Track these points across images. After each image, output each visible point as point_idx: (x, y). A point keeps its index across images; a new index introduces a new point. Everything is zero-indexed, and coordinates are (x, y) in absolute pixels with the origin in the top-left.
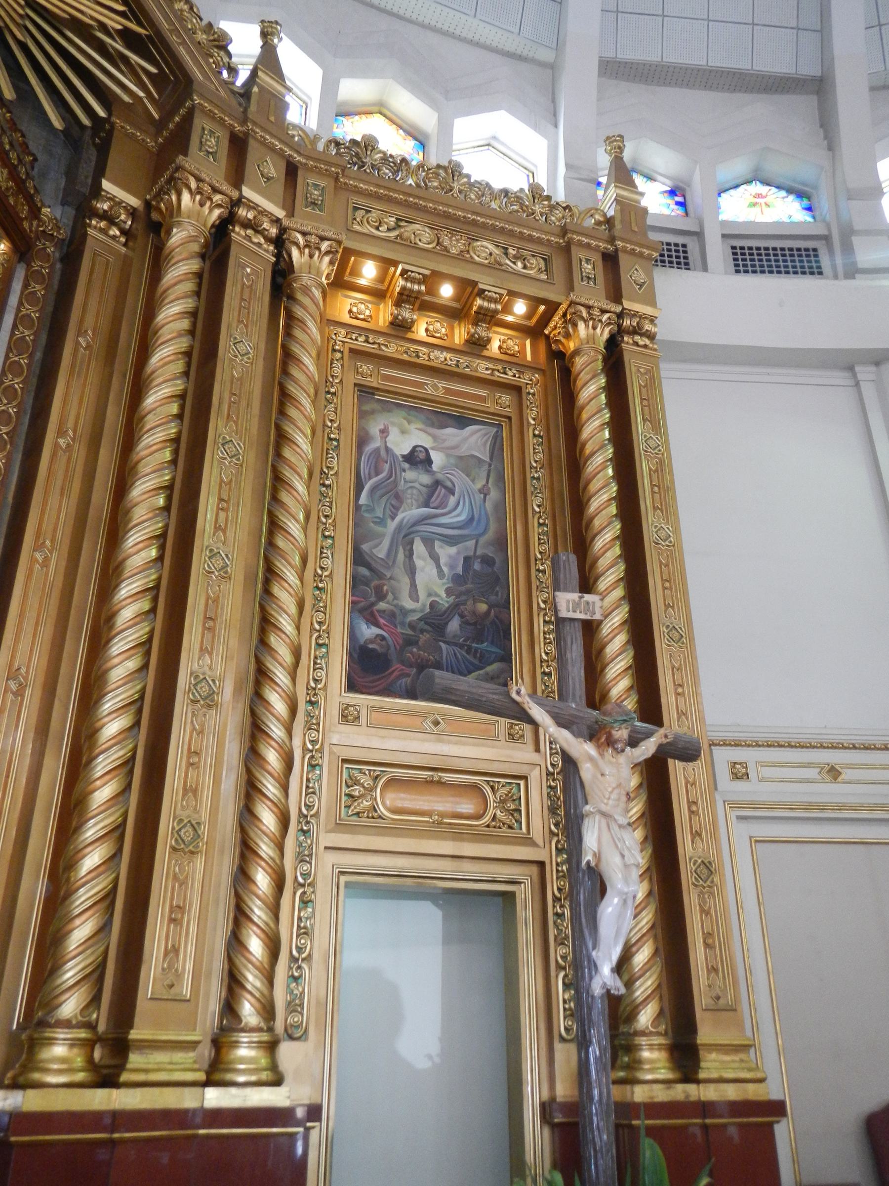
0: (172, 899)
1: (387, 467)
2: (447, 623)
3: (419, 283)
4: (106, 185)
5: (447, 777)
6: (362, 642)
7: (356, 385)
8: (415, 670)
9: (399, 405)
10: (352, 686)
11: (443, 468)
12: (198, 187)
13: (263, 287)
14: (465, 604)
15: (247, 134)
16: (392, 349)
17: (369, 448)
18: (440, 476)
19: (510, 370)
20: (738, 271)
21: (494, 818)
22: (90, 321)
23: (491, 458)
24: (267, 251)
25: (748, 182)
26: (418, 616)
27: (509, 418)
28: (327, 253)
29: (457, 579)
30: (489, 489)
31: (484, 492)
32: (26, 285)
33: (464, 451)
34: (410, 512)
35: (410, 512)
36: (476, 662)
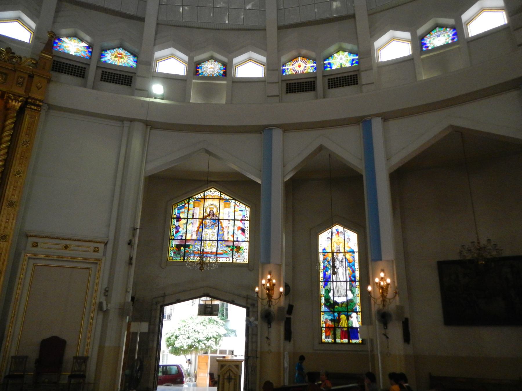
20: (101, 80)
25: (118, 48)
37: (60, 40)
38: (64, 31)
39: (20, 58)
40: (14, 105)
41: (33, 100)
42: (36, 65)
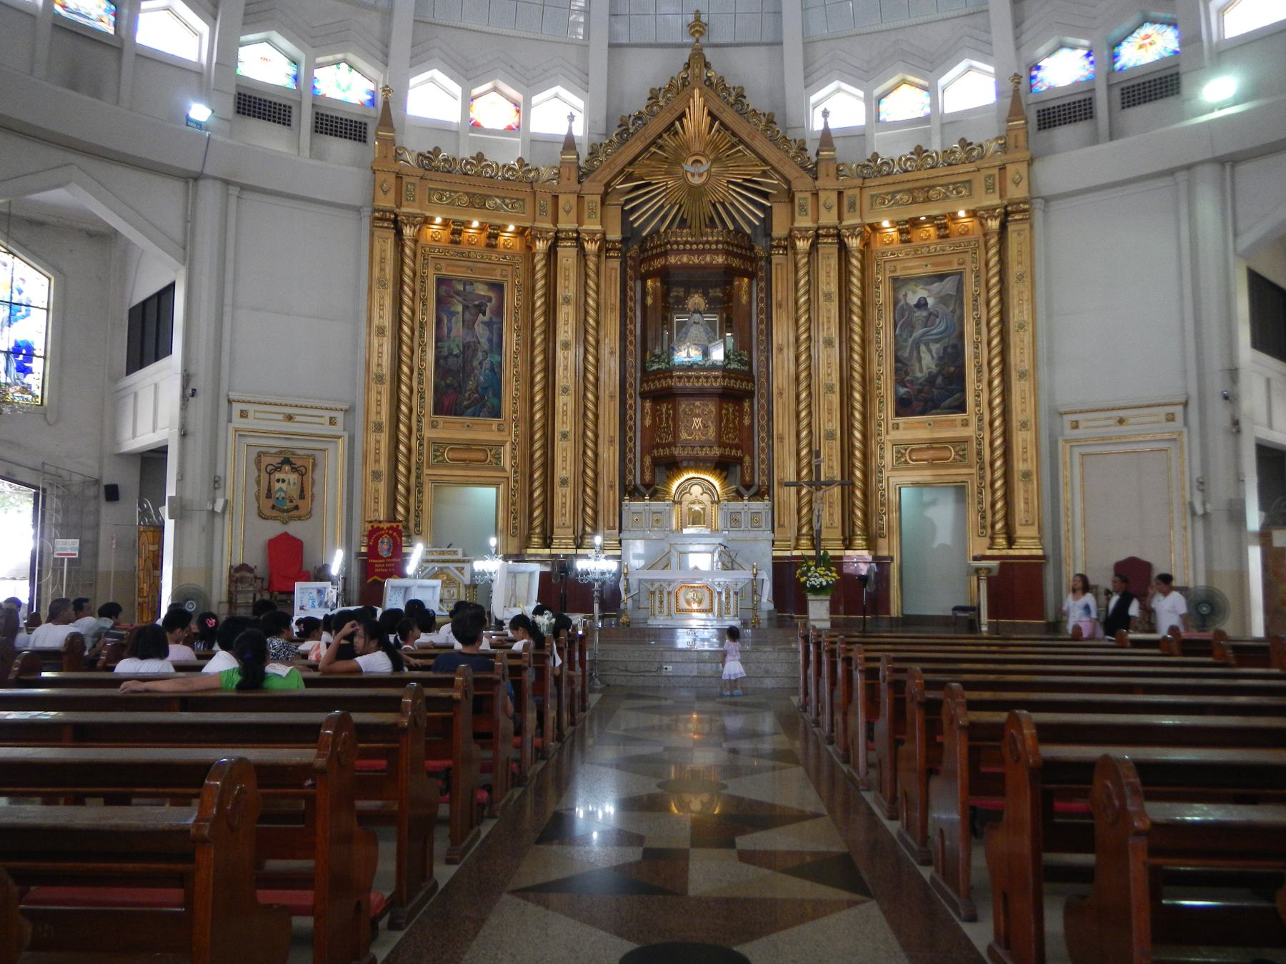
1: (907, 313)
4: (774, 234)
8: (922, 404)
9: (911, 279)
10: (898, 414)
11: (934, 304)
13: (834, 262)
17: (898, 307)
18: (932, 310)
21: (954, 459)
22: (779, 298)
25: (1140, 25)
29: (940, 359)
31: (953, 312)
32: (758, 285)
33: (943, 294)
34: (919, 332)
35: (919, 332)
37: (1038, 68)
38: (1042, 50)
39: (981, 146)
41: (1015, 206)
42: (1004, 148)
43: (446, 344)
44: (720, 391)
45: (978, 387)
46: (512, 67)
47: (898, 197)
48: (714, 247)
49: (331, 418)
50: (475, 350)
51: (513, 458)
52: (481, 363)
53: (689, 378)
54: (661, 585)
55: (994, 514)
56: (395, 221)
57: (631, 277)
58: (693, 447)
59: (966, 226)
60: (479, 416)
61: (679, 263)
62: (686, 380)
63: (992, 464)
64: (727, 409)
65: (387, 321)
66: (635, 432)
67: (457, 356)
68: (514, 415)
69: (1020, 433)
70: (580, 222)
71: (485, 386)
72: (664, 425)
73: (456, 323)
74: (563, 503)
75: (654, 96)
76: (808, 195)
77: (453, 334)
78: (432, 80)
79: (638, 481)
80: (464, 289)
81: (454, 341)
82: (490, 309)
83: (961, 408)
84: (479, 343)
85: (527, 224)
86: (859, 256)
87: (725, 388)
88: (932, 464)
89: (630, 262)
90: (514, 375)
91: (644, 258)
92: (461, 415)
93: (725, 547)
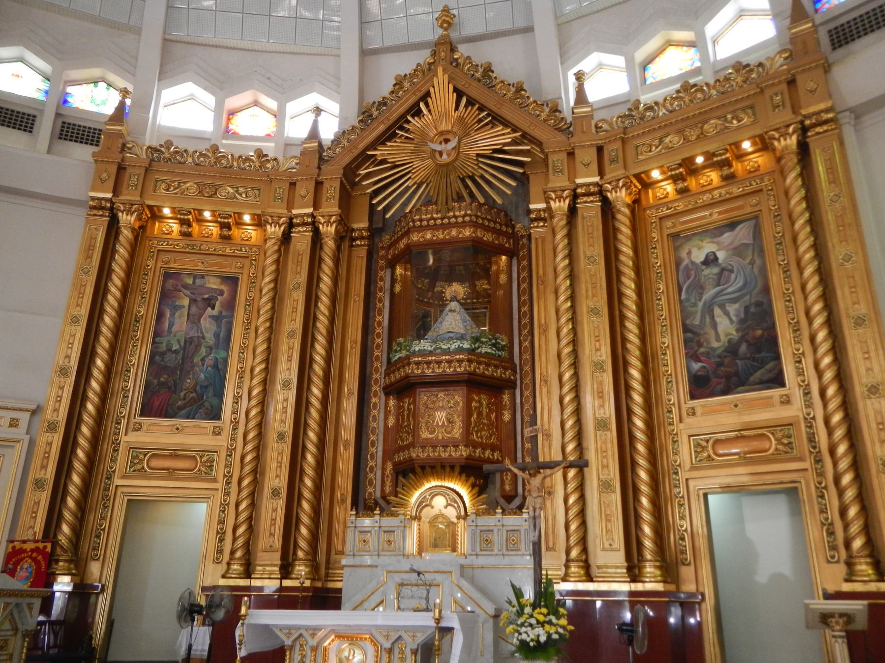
0: (605, 511)
1: (693, 273)
2: (738, 350)
3: (678, 168)
5: (745, 433)
6: (694, 372)
7: (668, 235)
8: (723, 380)
10: (693, 397)
11: (725, 259)
12: (556, 195)
14: (747, 334)
15: (573, 149)
16: (681, 206)
18: (724, 265)
19: (755, 181)
21: (777, 449)
23: (754, 239)
24: (596, 202)
26: (722, 349)
27: (760, 210)
28: (623, 186)
29: (742, 321)
30: (755, 261)
31: (752, 263)
32: (519, 264)
33: (737, 243)
36: (759, 365)
39: (760, 65)
40: (786, 147)
43: (164, 340)
44: (466, 377)
45: (798, 350)
46: (269, 78)
47: (667, 140)
48: (460, 220)
49: (13, 420)
50: (198, 346)
51: (226, 466)
52: (203, 360)
53: (428, 363)
54: (301, 635)
55: (846, 527)
56: (112, 209)
57: (382, 267)
58: (434, 447)
59: (756, 162)
60: (193, 418)
61: (422, 240)
62: (425, 366)
63: (832, 451)
64: (479, 401)
65: (84, 312)
66: (377, 436)
67: (176, 352)
68: (235, 416)
69: (869, 402)
70: (316, 205)
71: (206, 384)
72: (406, 423)
73: (181, 316)
74: (272, 520)
75: (399, 83)
76: (565, 155)
77: (174, 329)
78: (192, 98)
79: (378, 494)
80: (194, 282)
81: (175, 336)
82: (221, 303)
83: (778, 381)
84: (204, 338)
85: (259, 212)
86: (627, 211)
87: (470, 373)
88: (745, 459)
89: (383, 253)
90: (238, 371)
91: (391, 243)
92: (173, 416)
93: (419, 573)
